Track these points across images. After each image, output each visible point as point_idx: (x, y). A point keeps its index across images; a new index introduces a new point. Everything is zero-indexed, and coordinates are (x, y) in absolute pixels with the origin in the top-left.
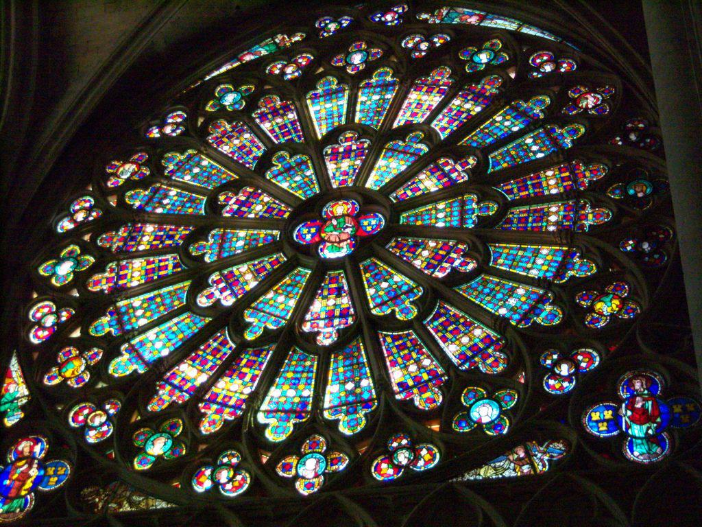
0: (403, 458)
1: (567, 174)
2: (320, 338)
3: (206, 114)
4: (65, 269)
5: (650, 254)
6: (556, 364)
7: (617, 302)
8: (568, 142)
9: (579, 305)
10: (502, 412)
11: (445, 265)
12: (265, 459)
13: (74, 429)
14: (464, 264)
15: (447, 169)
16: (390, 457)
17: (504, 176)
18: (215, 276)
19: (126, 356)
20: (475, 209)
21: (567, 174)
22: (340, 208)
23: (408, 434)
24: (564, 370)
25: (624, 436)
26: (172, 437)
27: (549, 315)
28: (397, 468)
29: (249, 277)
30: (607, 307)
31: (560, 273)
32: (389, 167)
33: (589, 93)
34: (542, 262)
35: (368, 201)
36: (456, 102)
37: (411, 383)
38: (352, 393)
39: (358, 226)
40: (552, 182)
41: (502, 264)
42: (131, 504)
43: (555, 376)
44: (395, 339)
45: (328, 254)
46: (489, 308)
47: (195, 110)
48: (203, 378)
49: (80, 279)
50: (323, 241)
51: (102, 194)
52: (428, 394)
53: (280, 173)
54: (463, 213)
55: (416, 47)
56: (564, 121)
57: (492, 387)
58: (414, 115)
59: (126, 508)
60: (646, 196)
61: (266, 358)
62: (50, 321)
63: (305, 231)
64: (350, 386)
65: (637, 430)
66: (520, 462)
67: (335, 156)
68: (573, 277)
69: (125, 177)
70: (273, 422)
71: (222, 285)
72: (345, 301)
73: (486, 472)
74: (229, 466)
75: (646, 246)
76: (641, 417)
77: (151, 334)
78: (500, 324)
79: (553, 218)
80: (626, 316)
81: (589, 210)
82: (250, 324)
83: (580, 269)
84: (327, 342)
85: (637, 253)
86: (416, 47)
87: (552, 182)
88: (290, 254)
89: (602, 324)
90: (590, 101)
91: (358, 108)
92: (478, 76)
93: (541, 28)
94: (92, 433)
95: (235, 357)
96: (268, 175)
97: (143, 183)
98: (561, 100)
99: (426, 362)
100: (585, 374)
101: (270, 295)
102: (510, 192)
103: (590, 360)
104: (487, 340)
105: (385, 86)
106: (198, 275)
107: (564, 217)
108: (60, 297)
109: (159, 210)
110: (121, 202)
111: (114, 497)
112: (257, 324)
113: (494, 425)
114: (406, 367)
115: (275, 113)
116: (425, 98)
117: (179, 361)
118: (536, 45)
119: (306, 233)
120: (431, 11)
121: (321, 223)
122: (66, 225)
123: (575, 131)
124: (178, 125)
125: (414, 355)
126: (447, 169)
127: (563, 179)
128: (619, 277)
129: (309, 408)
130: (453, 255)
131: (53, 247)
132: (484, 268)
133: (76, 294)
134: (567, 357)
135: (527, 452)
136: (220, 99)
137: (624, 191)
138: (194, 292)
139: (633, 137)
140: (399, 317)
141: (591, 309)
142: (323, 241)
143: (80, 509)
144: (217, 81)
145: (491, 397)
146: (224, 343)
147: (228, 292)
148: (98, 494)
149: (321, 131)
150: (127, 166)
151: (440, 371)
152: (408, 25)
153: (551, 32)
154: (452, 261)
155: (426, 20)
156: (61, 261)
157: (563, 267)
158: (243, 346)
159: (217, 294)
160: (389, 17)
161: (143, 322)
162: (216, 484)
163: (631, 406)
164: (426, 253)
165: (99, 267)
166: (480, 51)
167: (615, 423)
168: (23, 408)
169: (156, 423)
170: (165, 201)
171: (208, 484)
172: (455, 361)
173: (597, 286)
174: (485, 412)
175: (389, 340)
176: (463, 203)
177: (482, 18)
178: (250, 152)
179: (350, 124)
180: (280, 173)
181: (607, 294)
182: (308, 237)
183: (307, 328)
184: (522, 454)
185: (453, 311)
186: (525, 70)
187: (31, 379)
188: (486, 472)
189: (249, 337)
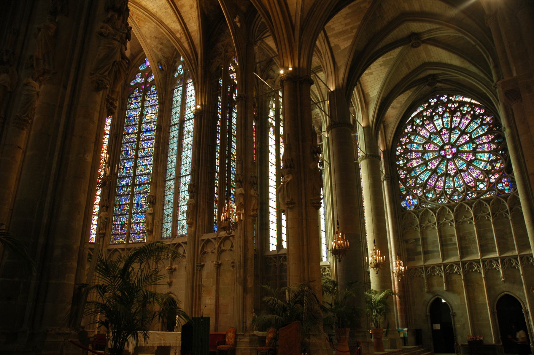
0: (470, 195)
1: (487, 137)
2: (451, 174)
3: (415, 125)
4: (401, 162)
5: (504, 154)
6: (491, 176)
7: (500, 164)
8: (486, 131)
9: (493, 165)
10: (484, 186)
11: (469, 158)
12: (448, 196)
13: (415, 194)
14: (472, 158)
15: (465, 137)
16: (468, 195)
17: (476, 138)
18: (429, 163)
19: (419, 179)
20: (472, 146)
21: (487, 137)
22: (447, 147)
23: (470, 191)
24: (493, 177)
25: (504, 189)
26: (432, 194)
27: (489, 167)
28: (470, 197)
29: (435, 162)
30: (498, 165)
31: (489, 159)
32: (454, 137)
33: (488, 117)
34: (485, 157)
35: (453, 145)
36: (463, 120)
37: (468, 182)
38: (459, 184)
39: (451, 150)
40: (484, 139)
41: (479, 158)
42: (429, 206)
43: (492, 179)
44: (464, 173)
45: (448, 157)
46: (478, 166)
47: (413, 125)
48: (434, 183)
49: (405, 164)
50: (446, 154)
51: (401, 145)
52: (472, 183)
53: (434, 139)
54: (470, 147)
55: (451, 107)
56: (484, 125)
57: (482, 181)
58: (455, 124)
59: (429, 206)
60: (502, 141)
61: (443, 178)
62: (403, 173)
63: (442, 152)
64: (458, 183)
65: (506, 188)
66: (489, 194)
67: (443, 134)
68: (491, 160)
69: (404, 141)
70: (448, 190)
71: (431, 164)
72: (453, 166)
73: (484, 197)
74: (443, 198)
75: (503, 152)
76: (506, 185)
77: (422, 175)
78: (480, 170)
79: (486, 147)
80: (501, 167)
81: (492, 145)
82: (438, 172)
83: (493, 158)
84: (453, 175)
85: (502, 154)
86: (451, 107)
87: (484, 139)
88: (442, 158)
89: (498, 169)
90: (488, 119)
91: (444, 122)
92: (465, 114)
93: (476, 100)
94: (418, 194)
95: (438, 179)
96: (432, 140)
97: (408, 143)
98: (483, 120)
99: (470, 178)
100: (497, 178)
101: (440, 166)
102: (477, 141)
103: (497, 176)
104: (479, 173)
105: (447, 117)
106: (426, 163)
107: (488, 147)
108: (402, 168)
109: (414, 149)
110: (406, 148)
111: (426, 205)
112: (440, 172)
113: (483, 188)
114: (467, 179)
115: (428, 124)
116: (456, 120)
117: (429, 180)
118: (476, 105)
119: (442, 153)
120: (452, 96)
121: (445, 150)
122: (397, 153)
123: (487, 127)
124: (410, 128)
125: (468, 176)
126: (465, 137)
127: (487, 138)
128: (499, 159)
129: (453, 187)
130: (470, 156)
131: (397, 158)
132: (476, 159)
133: (405, 167)
134: (493, 175)
135: (490, 193)
136: (416, 121)
137: (498, 141)
138: (427, 166)
139: (498, 128)
140: (463, 169)
141: (495, 166)
142: (446, 154)
143: (422, 207)
144: (414, 117)
145: (482, 183)
146: (435, 176)
147: (432, 166)
148: (423, 204)
149: (439, 129)
150: (404, 139)
151: (473, 179)
152: (449, 101)
153: (478, 101)
154: (470, 157)
155: (451, 99)
156: (399, 161)
157: (489, 158)
158: (439, 177)
159: (430, 166)
160: (444, 98)
161: (419, 172)
162: (442, 202)
163: (505, 184)
164: (465, 156)
165: (407, 162)
166: (464, 107)
167: (503, 186)
168: (405, 190)
169: (429, 192)
170: (414, 146)
171: (440, 201)
172: (475, 177)
173: (496, 161)
174: (481, 186)
175: (463, 173)
176: (469, 145)
177: (463, 98)
178: (426, 134)
179: (444, 128)
180: (434, 139)
181: (498, 163)
182: (443, 154)
183: (448, 172)
184: (489, 193)
185: (472, 167)
186: (475, 112)
187: (405, 185)
188: (484, 197)
189: (439, 174)
